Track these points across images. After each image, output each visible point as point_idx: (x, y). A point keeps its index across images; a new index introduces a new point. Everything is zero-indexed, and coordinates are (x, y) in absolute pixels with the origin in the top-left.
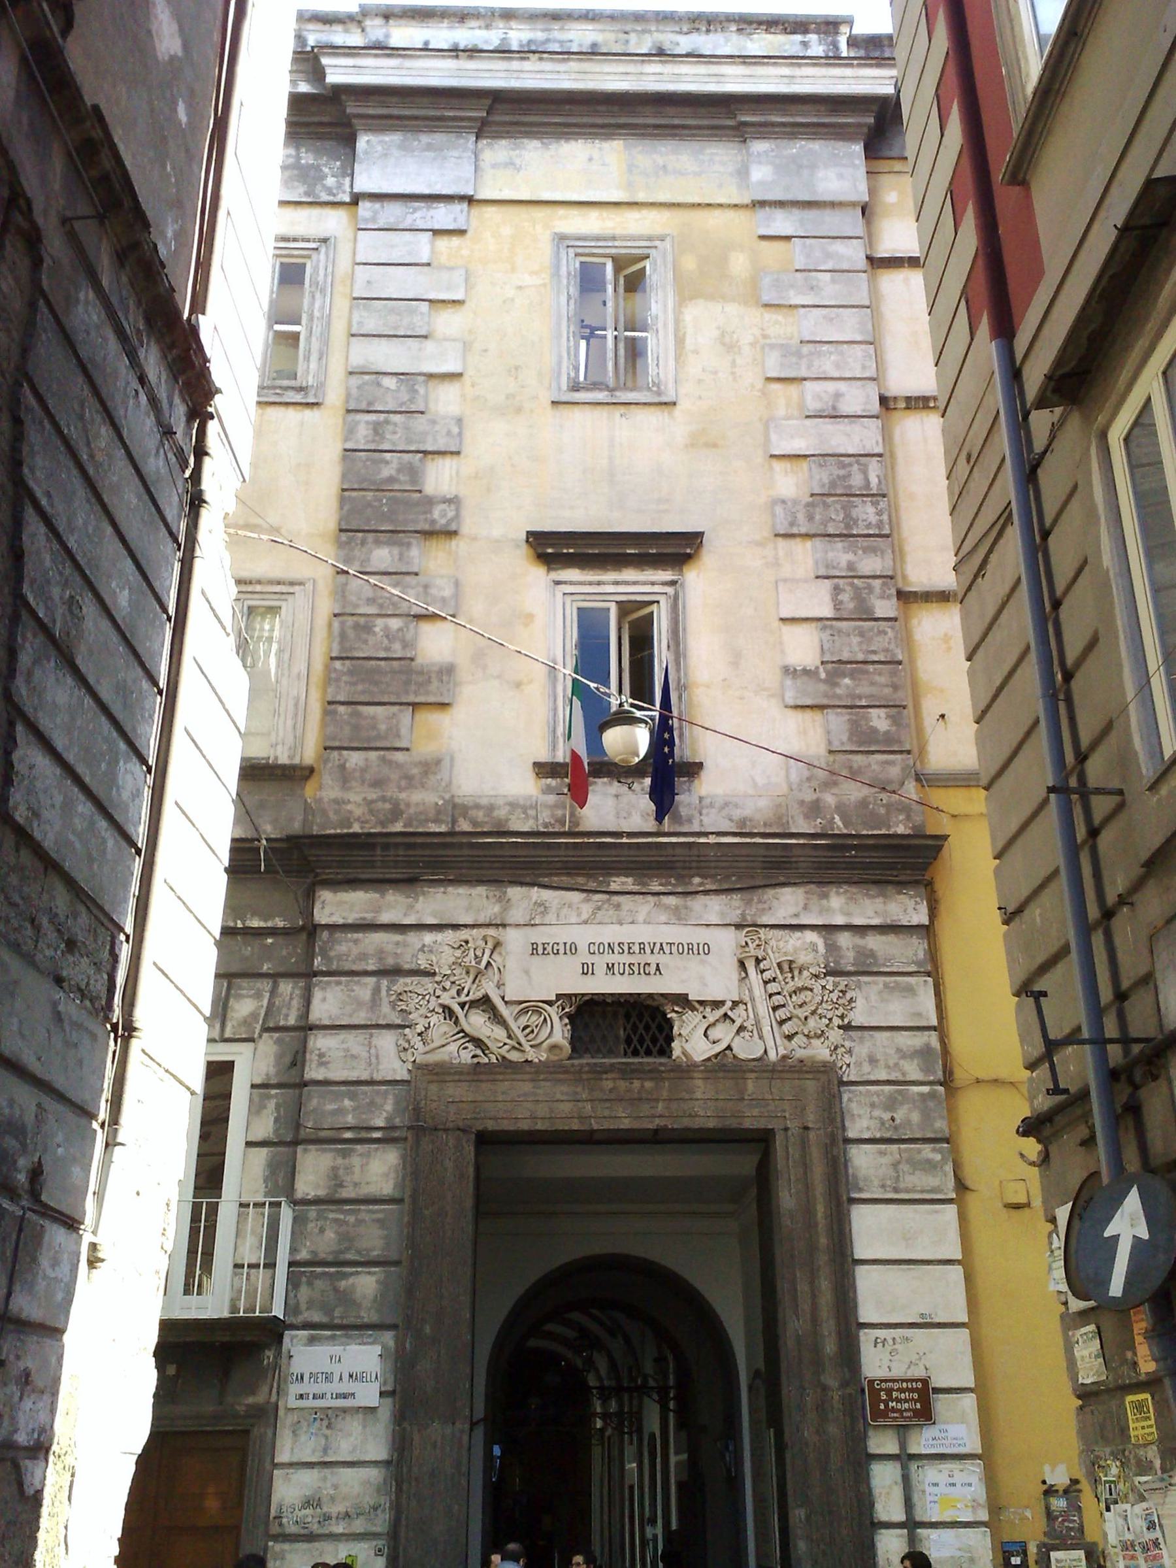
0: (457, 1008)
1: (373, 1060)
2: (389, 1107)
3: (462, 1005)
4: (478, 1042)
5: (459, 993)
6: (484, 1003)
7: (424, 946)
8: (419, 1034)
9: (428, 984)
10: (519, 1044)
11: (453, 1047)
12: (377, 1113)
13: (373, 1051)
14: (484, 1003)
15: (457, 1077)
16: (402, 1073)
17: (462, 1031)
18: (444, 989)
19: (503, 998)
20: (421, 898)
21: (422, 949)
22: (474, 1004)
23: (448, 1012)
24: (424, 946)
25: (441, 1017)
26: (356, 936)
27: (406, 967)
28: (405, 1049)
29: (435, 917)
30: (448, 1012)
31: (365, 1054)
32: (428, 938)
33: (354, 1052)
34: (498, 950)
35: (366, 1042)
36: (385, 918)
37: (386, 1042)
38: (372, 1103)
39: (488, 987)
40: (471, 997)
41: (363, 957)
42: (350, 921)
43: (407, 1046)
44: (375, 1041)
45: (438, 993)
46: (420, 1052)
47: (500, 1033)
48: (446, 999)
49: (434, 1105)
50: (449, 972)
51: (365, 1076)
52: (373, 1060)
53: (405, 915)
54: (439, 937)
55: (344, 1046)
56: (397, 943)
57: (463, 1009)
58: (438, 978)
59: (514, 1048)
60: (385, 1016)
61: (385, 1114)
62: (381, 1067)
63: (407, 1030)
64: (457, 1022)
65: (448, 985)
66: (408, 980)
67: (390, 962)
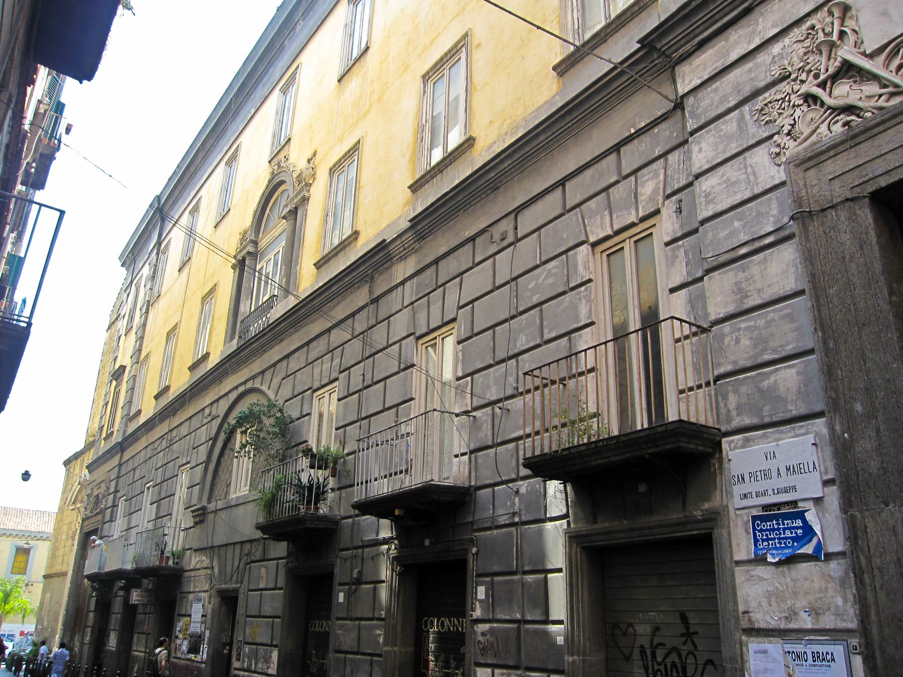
0: (818, 92)
1: (752, 178)
2: (775, 212)
3: (823, 85)
4: (849, 109)
5: (816, 76)
6: (847, 70)
7: (774, 57)
8: (789, 134)
9: (785, 87)
10: (896, 86)
11: (823, 128)
12: (765, 221)
13: (749, 170)
14: (847, 71)
15: (832, 153)
16: (779, 175)
17: (829, 108)
18: (802, 82)
19: (863, 54)
20: (760, 20)
21: (773, 62)
22: (835, 78)
23: (810, 99)
24: (774, 57)
25: (805, 108)
26: (714, 86)
27: (762, 84)
28: (778, 154)
29: (777, 26)
30: (810, 99)
31: (744, 177)
32: (776, 49)
33: (734, 179)
34: (849, 15)
35: (742, 166)
36: (734, 56)
37: (760, 156)
38: (759, 214)
39: (847, 52)
40: (831, 70)
41: (724, 98)
42: (706, 77)
43: (778, 150)
44: (749, 161)
45: (796, 88)
46: (792, 148)
47: (872, 88)
48: (804, 89)
49: (815, 190)
50: (802, 64)
51: (747, 195)
52: (752, 178)
53: (749, 43)
54: (787, 41)
55: (725, 178)
56: (750, 70)
57: (825, 90)
58: (793, 76)
59: (892, 95)
60: (754, 135)
61: (772, 219)
62: (759, 181)
63: (776, 138)
64: (823, 104)
65: (803, 76)
66: (767, 95)
67: (747, 91)
